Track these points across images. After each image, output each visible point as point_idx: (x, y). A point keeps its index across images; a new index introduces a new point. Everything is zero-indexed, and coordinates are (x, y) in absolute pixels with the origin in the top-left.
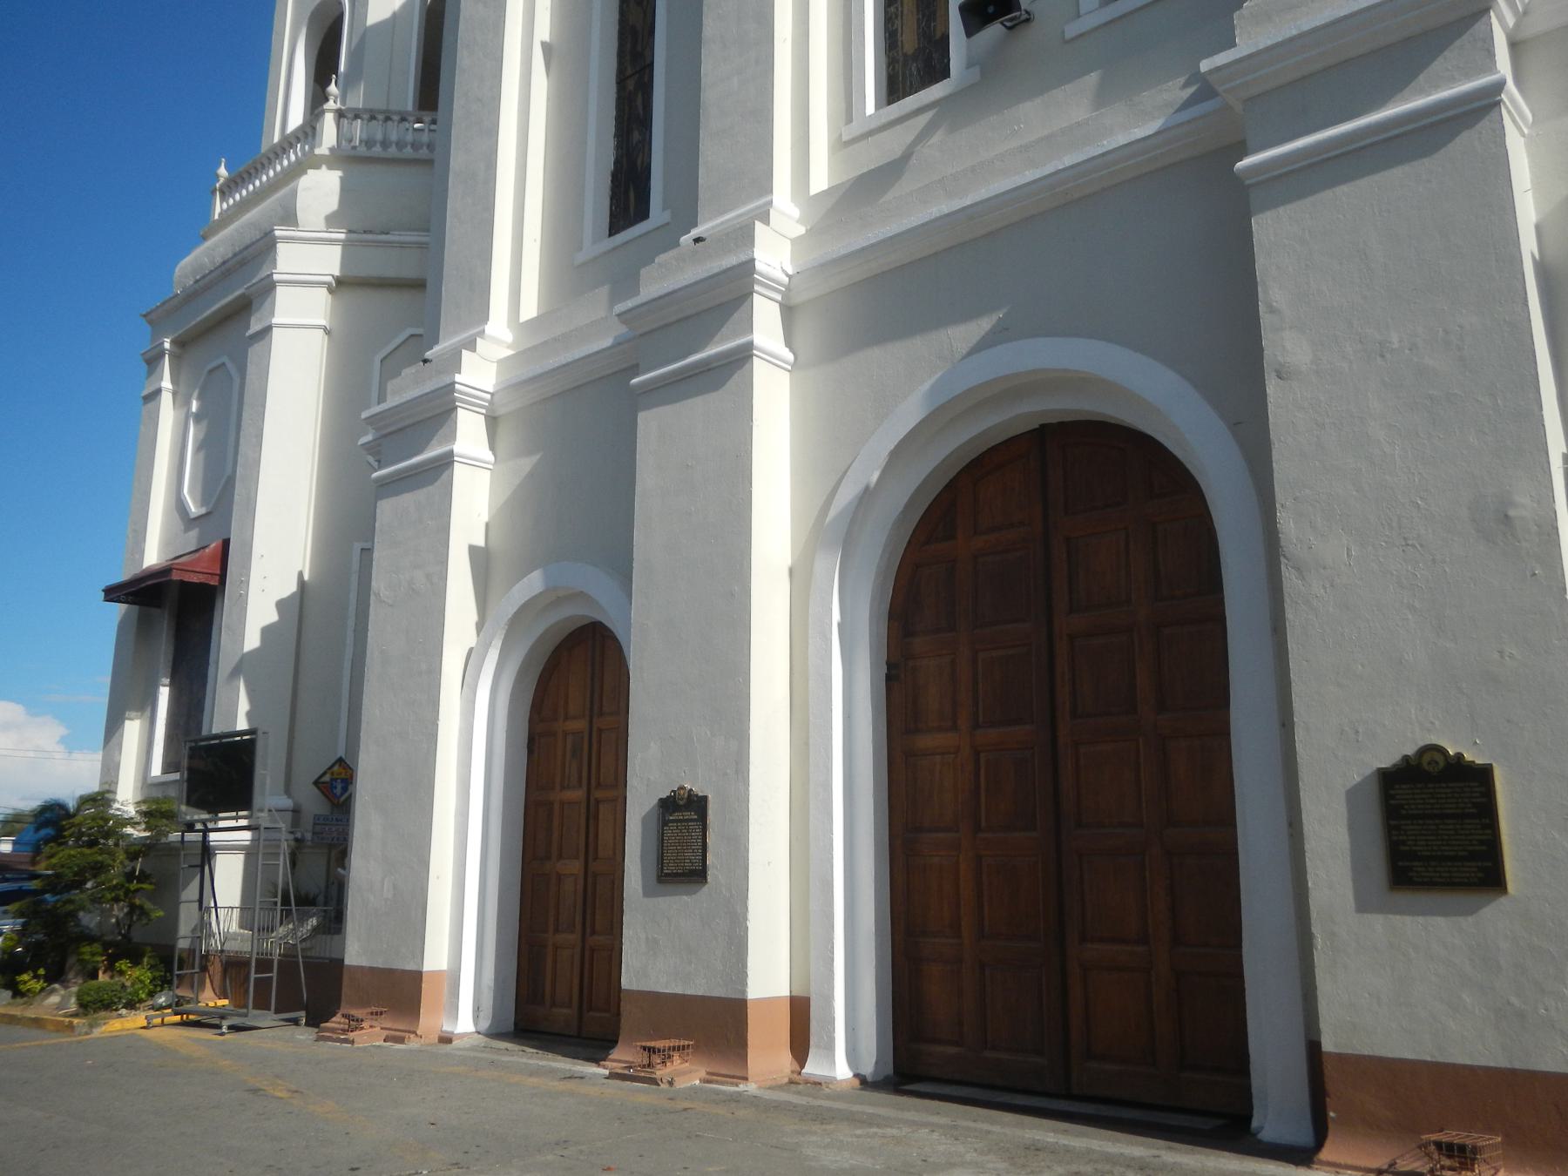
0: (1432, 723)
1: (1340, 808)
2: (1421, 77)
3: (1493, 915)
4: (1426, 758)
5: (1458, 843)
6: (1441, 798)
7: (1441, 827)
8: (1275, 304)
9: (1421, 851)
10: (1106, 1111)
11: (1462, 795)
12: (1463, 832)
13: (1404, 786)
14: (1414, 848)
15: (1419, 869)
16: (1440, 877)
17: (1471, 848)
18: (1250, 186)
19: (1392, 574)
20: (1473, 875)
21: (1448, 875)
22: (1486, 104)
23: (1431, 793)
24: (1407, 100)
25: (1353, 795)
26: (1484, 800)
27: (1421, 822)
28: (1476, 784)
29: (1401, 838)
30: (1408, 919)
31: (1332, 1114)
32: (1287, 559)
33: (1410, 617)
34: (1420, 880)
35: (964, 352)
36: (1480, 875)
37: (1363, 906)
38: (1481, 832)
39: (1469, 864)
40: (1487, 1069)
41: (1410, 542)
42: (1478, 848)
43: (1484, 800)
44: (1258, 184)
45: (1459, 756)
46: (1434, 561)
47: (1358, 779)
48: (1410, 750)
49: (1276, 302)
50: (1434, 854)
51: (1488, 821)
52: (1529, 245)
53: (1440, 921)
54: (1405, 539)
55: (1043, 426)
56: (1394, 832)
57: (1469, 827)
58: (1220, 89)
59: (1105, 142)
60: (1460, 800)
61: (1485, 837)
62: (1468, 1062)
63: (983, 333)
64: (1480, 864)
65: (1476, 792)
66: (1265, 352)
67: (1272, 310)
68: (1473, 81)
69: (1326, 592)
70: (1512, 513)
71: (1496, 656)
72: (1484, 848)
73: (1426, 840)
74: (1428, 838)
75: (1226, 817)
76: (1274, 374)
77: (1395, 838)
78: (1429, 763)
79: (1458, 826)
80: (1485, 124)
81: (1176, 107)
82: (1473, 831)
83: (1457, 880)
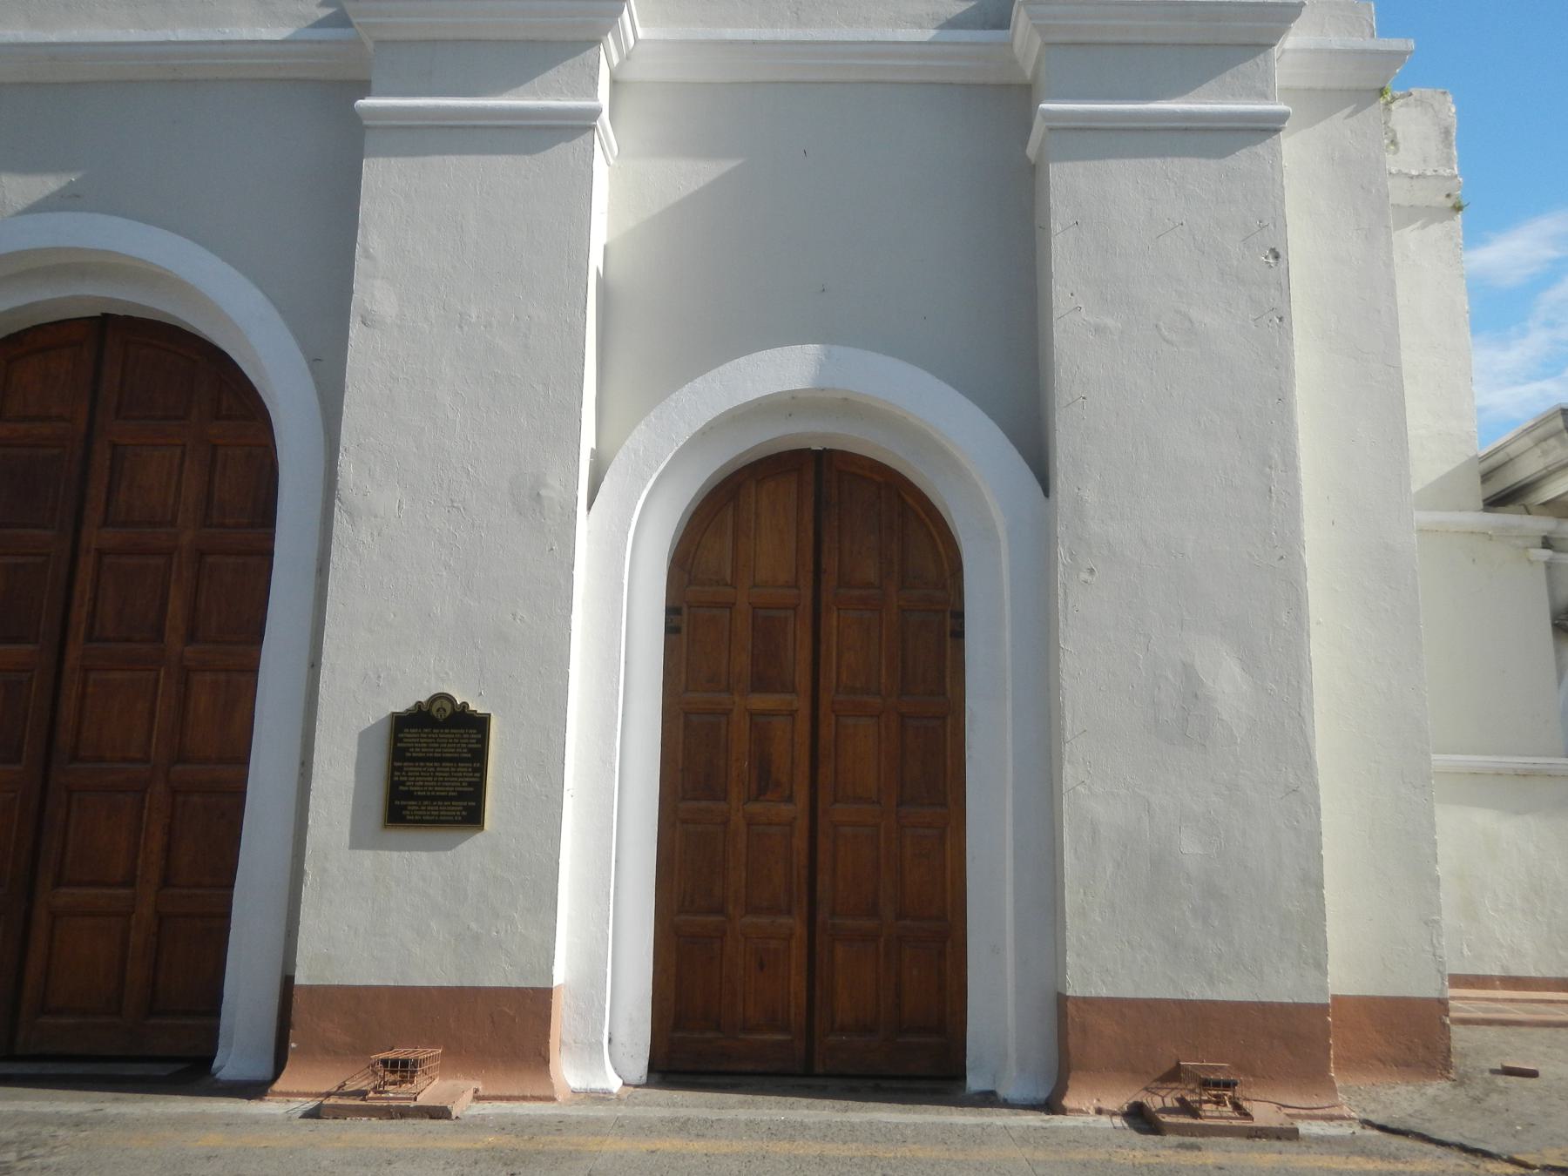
0: (447, 674)
1: (352, 749)
2: (536, 80)
3: (470, 849)
4: (437, 705)
5: (449, 784)
7: (438, 769)
8: (371, 250)
9: (417, 791)
10: (51, 1068)
12: (455, 774)
13: (413, 731)
14: (411, 788)
15: (414, 808)
16: (431, 815)
17: (461, 789)
18: (367, 127)
19: (435, 532)
20: (458, 813)
21: (437, 813)
22: (579, 125)
23: (436, 739)
24: (520, 97)
25: (364, 736)
26: (479, 746)
27: (422, 764)
28: (475, 731)
29: (401, 779)
30: (395, 854)
31: (293, 1045)
32: (342, 503)
33: (444, 573)
34: (412, 818)
35: (19, 208)
36: (464, 813)
37: (357, 843)
38: (471, 774)
39: (456, 803)
40: (441, 988)
41: (455, 505)
42: (465, 789)
43: (479, 746)
44: (375, 127)
45: (465, 705)
46: (473, 525)
47: (372, 722)
48: (424, 697)
49: (373, 248)
50: (429, 793)
51: (478, 765)
52: (596, 261)
53: (424, 856)
54: (452, 501)
55: (106, 316)
56: (396, 773)
58: (354, 21)
59: (227, 31)
60: (459, 745)
62: (425, 984)
63: (47, 192)
64: (465, 804)
65: (473, 739)
66: (354, 295)
67: (368, 255)
68: (577, 100)
69: (373, 540)
70: (543, 492)
71: (510, 618)
72: (471, 789)
73: (424, 781)
74: (425, 779)
75: (240, 757)
76: (360, 318)
77: (396, 779)
78: (438, 710)
79: (453, 769)
80: (579, 142)
81: (310, 23)
83: (444, 818)
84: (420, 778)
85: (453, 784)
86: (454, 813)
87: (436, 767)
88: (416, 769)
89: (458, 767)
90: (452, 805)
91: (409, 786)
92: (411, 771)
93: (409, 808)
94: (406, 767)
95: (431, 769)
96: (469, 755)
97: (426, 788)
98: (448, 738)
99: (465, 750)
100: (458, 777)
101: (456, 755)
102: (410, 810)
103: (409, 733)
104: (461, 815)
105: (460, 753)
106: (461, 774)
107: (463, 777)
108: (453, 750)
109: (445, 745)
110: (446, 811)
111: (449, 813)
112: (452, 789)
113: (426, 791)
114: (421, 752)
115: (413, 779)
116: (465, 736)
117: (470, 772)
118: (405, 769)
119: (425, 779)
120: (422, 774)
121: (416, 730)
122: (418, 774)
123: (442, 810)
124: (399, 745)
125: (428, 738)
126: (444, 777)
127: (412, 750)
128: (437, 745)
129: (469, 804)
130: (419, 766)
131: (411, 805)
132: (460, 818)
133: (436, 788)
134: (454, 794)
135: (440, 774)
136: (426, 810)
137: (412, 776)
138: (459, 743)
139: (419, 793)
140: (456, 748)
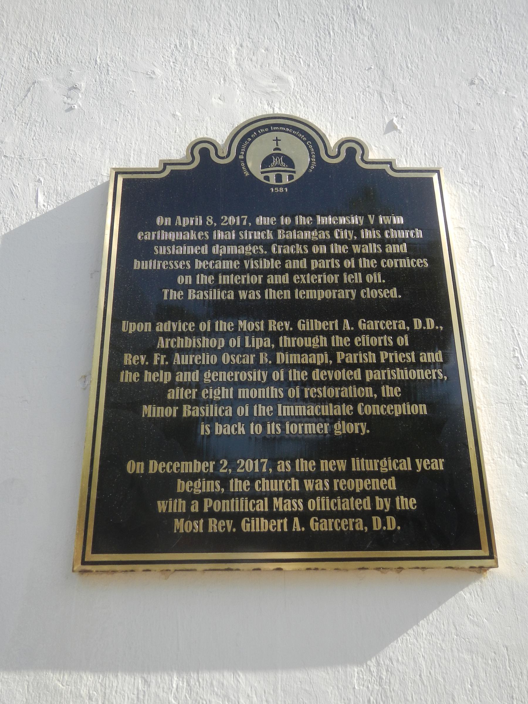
0: (279, 78)
6: (293, 257)
9: (210, 420)
11: (356, 249)
13: (187, 221)
14: (187, 411)
17: (377, 410)
20: (382, 503)
21: (298, 505)
23: (267, 245)
26: (423, 263)
27: (223, 326)
28: (399, 220)
29: (149, 377)
34: (198, 526)
38: (411, 357)
39: (370, 465)
50: (256, 429)
51: (431, 324)
56: (128, 359)
57: (375, 341)
60: (349, 263)
61: (420, 374)
64: (405, 465)
65: (398, 241)
78: (267, 162)
79: (339, 341)
82: (384, 355)
84: (224, 376)
85: (347, 392)
86: (366, 504)
87: (275, 336)
88: (206, 342)
89: (358, 333)
90: (349, 474)
91: (179, 403)
92: (183, 351)
93: (182, 486)
94: (165, 335)
95: (259, 343)
96: (393, 293)
97: (243, 411)
98: (310, 243)
99: (376, 278)
100: (364, 367)
101: (343, 294)
102: (189, 497)
103: (173, 228)
104: (393, 511)
105: (358, 287)
106: (371, 358)
107: (378, 366)
108: (333, 279)
109: (303, 264)
110: (332, 494)
111: (346, 505)
112: (347, 410)
113: (246, 421)
114: (216, 286)
115: (194, 376)
116: (367, 234)
117: (403, 349)
118: (162, 343)
119: (243, 376)
120: (226, 359)
121: (199, 221)
122: (214, 359)
123: (314, 494)
124: (137, 264)
125: (237, 242)
126: (310, 367)
127: (188, 280)
128: (275, 264)
129: (422, 464)
130: (212, 334)
131: (193, 477)
132: (392, 523)
133: (285, 410)
134: (352, 428)
135: (295, 359)
136: (253, 495)
137: (190, 368)
138: (350, 255)
139: (219, 430)
140: (342, 270)
